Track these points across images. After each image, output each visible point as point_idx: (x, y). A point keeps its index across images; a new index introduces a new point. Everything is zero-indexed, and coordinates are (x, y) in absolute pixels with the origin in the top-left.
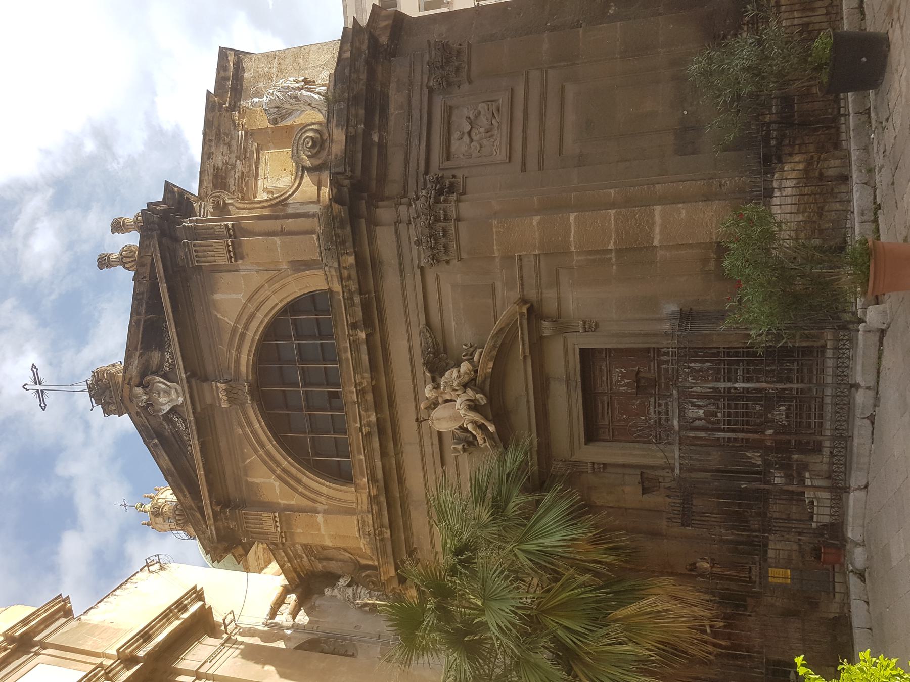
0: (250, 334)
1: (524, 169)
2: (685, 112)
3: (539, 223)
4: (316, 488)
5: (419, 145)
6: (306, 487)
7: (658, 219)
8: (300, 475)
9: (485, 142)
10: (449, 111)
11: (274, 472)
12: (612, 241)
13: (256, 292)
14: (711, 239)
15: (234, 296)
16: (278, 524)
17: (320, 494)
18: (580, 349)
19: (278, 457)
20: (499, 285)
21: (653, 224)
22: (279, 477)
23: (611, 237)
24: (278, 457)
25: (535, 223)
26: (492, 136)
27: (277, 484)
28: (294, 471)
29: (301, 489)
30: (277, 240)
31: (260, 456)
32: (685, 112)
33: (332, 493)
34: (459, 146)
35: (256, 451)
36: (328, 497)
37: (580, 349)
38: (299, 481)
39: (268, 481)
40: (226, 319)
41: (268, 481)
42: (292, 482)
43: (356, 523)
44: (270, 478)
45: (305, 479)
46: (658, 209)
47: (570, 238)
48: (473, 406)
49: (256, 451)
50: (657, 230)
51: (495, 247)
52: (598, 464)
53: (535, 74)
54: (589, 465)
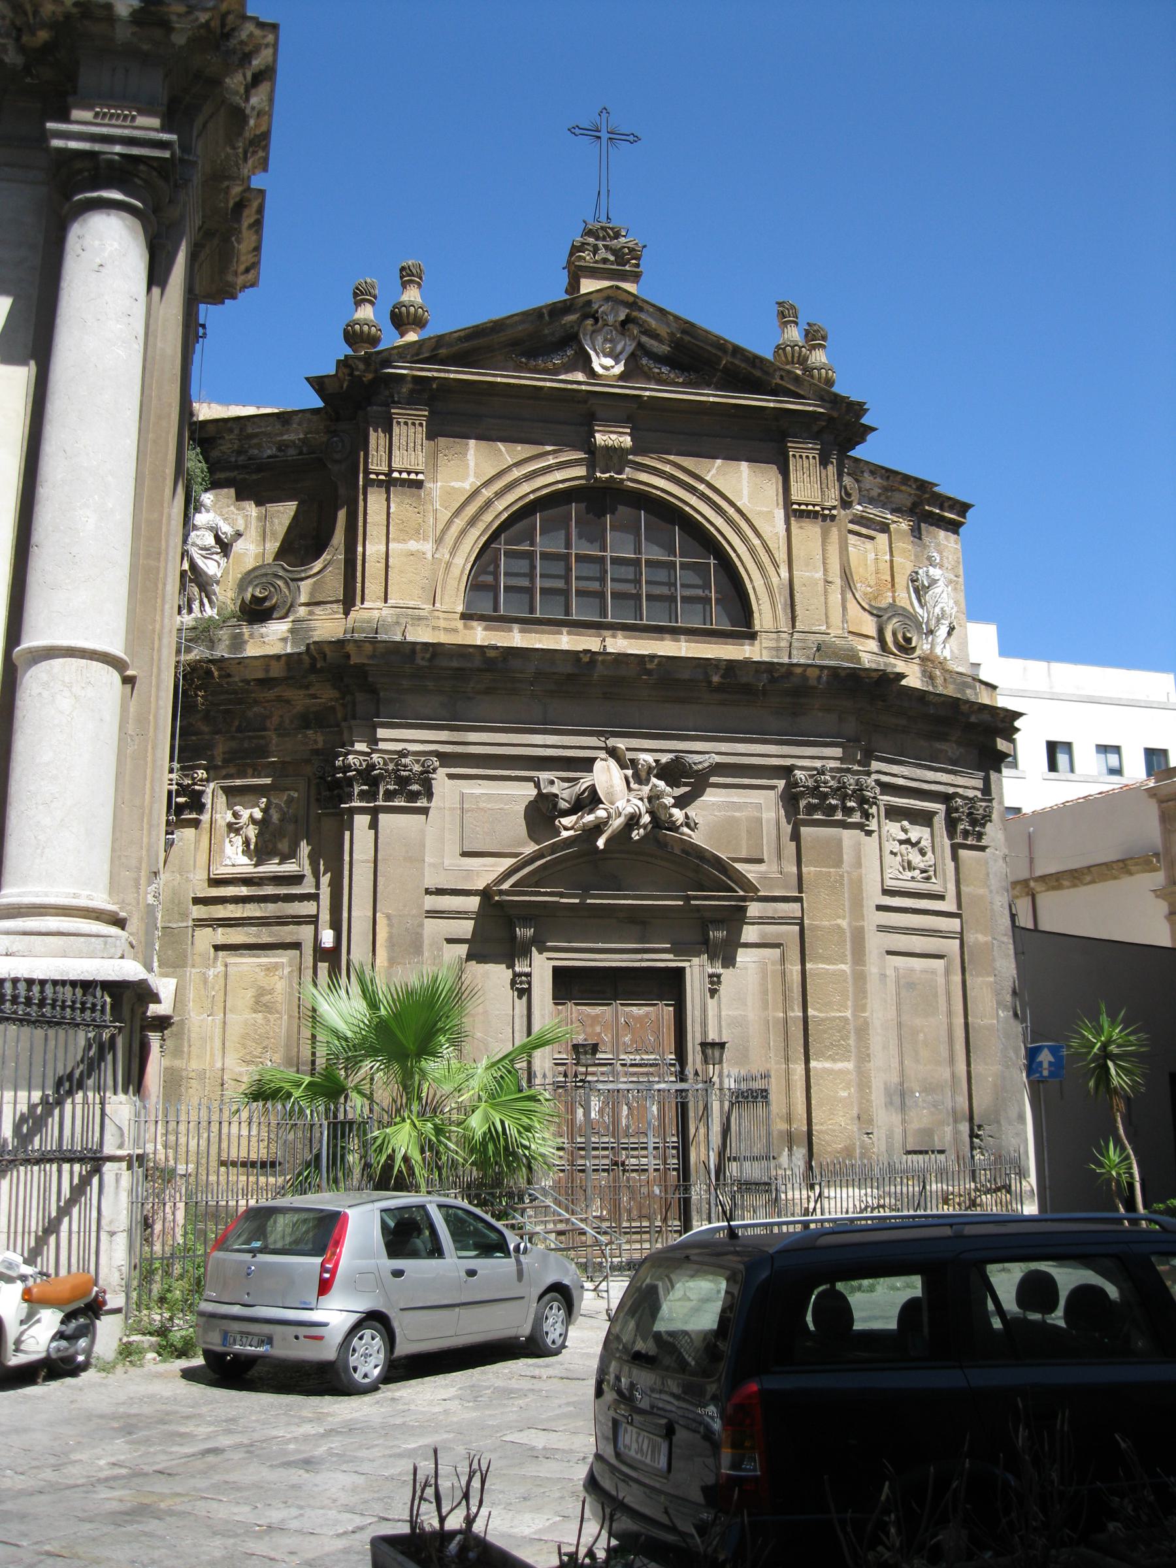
0: (693, 500)
1: (880, 908)
2: (917, 1094)
3: (839, 926)
4: (462, 547)
5: (903, 777)
6: (463, 532)
7: (839, 1066)
8: (481, 526)
9: (899, 858)
10: (924, 819)
11: (487, 484)
12: (816, 1013)
13: (748, 520)
14: (816, 1124)
15: (745, 492)
16: (404, 475)
17: (453, 552)
18: (683, 969)
19: (510, 498)
20: (762, 868)
21: (834, 1060)
22: (476, 493)
23: (821, 1011)
24: (510, 498)
25: (839, 921)
26: (904, 869)
27: (468, 484)
28: (488, 517)
29: (459, 523)
30: (819, 575)
31: (509, 468)
32: (917, 1094)
33: (456, 571)
34: (893, 829)
35: (518, 464)
36: (449, 565)
37: (683, 969)
38: (472, 522)
39: (472, 473)
40: (714, 471)
41: (472, 473)
42: (471, 510)
43: (411, 604)
44: (477, 476)
45: (475, 532)
46: (849, 1066)
47: (823, 962)
48: (633, 821)
49: (518, 464)
50: (828, 1065)
51: (812, 869)
52: (529, 983)
53: (954, 924)
54: (527, 970)
